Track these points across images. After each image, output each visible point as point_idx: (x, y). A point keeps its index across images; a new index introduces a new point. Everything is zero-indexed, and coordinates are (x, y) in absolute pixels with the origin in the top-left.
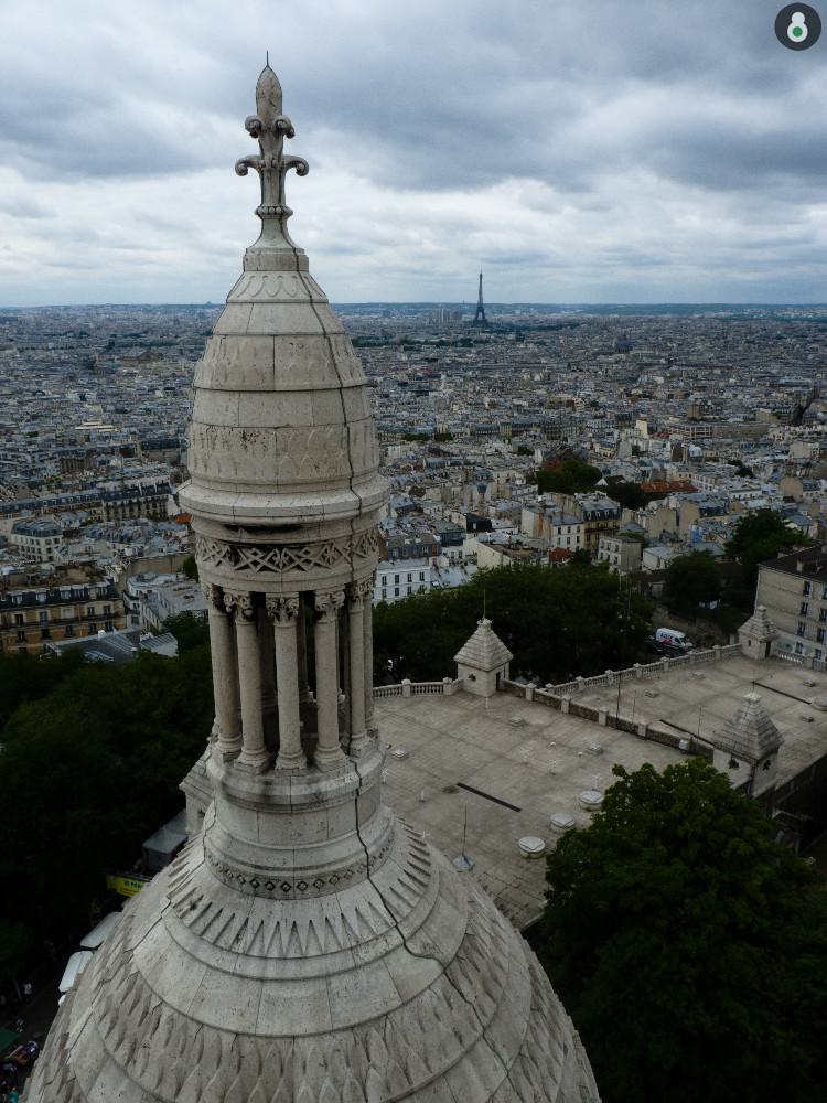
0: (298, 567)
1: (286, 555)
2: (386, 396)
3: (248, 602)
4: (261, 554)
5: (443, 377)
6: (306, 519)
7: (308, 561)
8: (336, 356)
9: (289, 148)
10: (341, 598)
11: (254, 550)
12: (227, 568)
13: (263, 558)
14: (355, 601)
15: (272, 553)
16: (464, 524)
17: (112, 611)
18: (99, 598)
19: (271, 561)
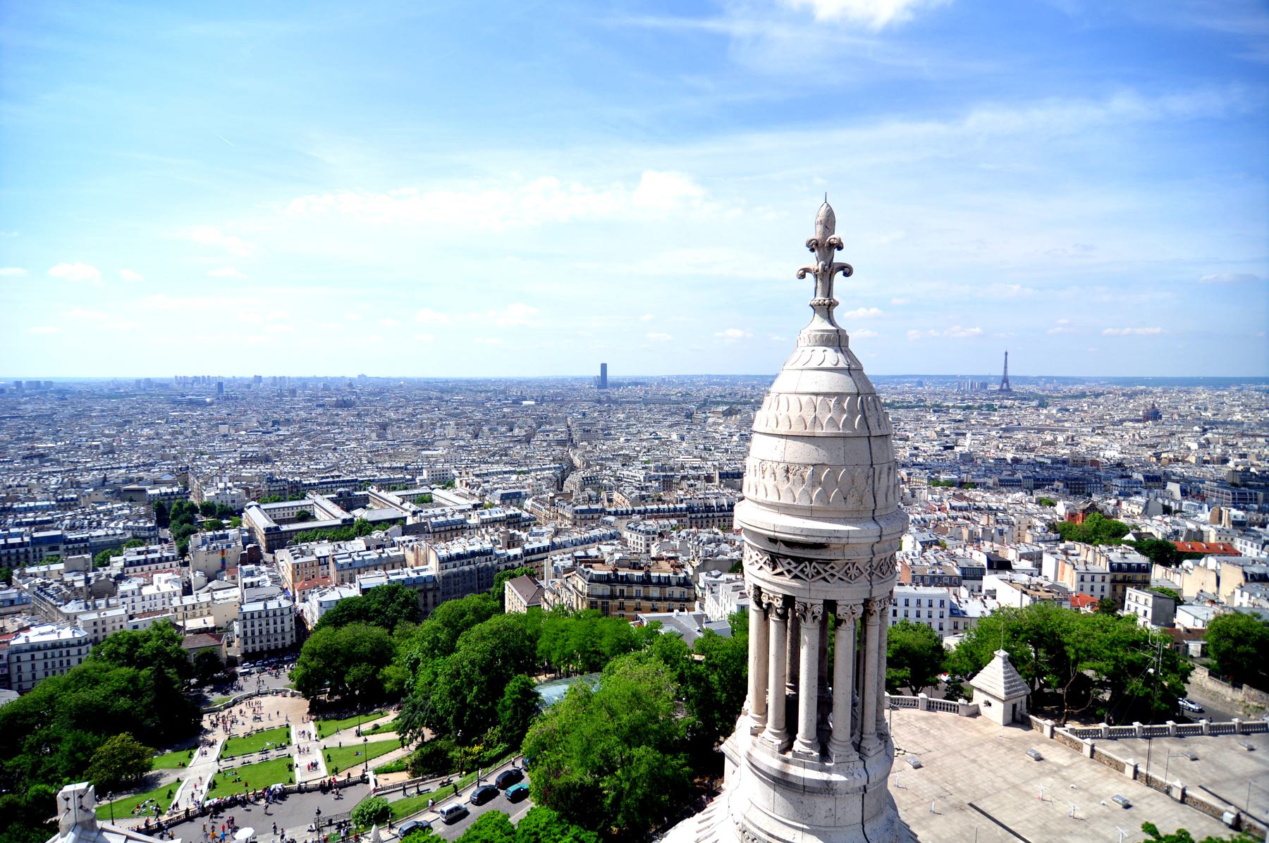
0: (824, 579)
1: (815, 567)
2: (916, 448)
3: (781, 602)
4: (794, 565)
5: (969, 435)
6: (833, 541)
7: (833, 575)
8: (867, 411)
9: (838, 257)
10: (860, 610)
11: (789, 560)
12: (767, 572)
13: (796, 568)
14: (872, 615)
15: (803, 565)
16: (984, 562)
17: (686, 596)
18: (678, 584)
19: (802, 571)
